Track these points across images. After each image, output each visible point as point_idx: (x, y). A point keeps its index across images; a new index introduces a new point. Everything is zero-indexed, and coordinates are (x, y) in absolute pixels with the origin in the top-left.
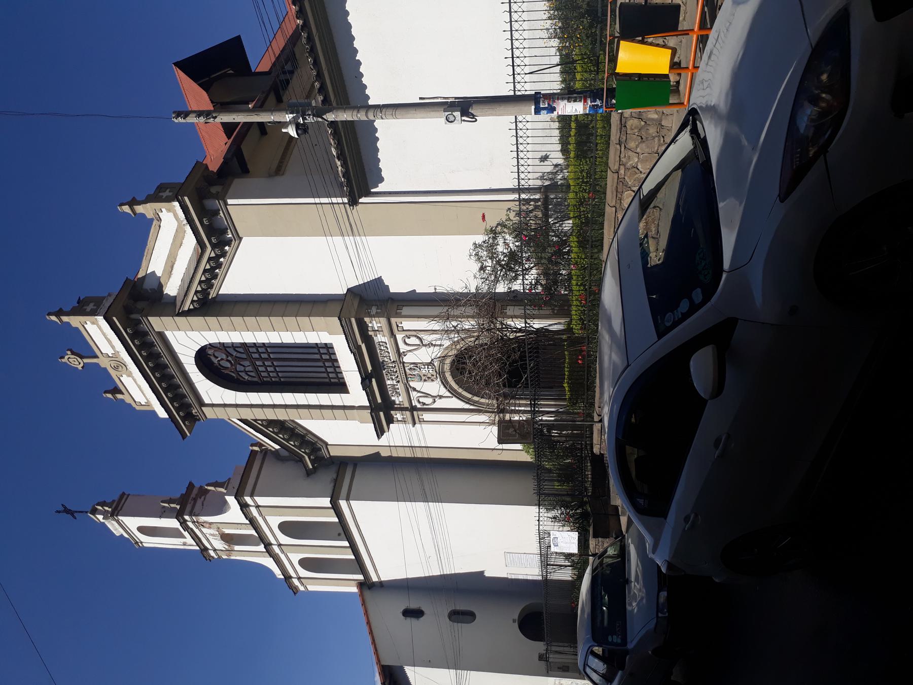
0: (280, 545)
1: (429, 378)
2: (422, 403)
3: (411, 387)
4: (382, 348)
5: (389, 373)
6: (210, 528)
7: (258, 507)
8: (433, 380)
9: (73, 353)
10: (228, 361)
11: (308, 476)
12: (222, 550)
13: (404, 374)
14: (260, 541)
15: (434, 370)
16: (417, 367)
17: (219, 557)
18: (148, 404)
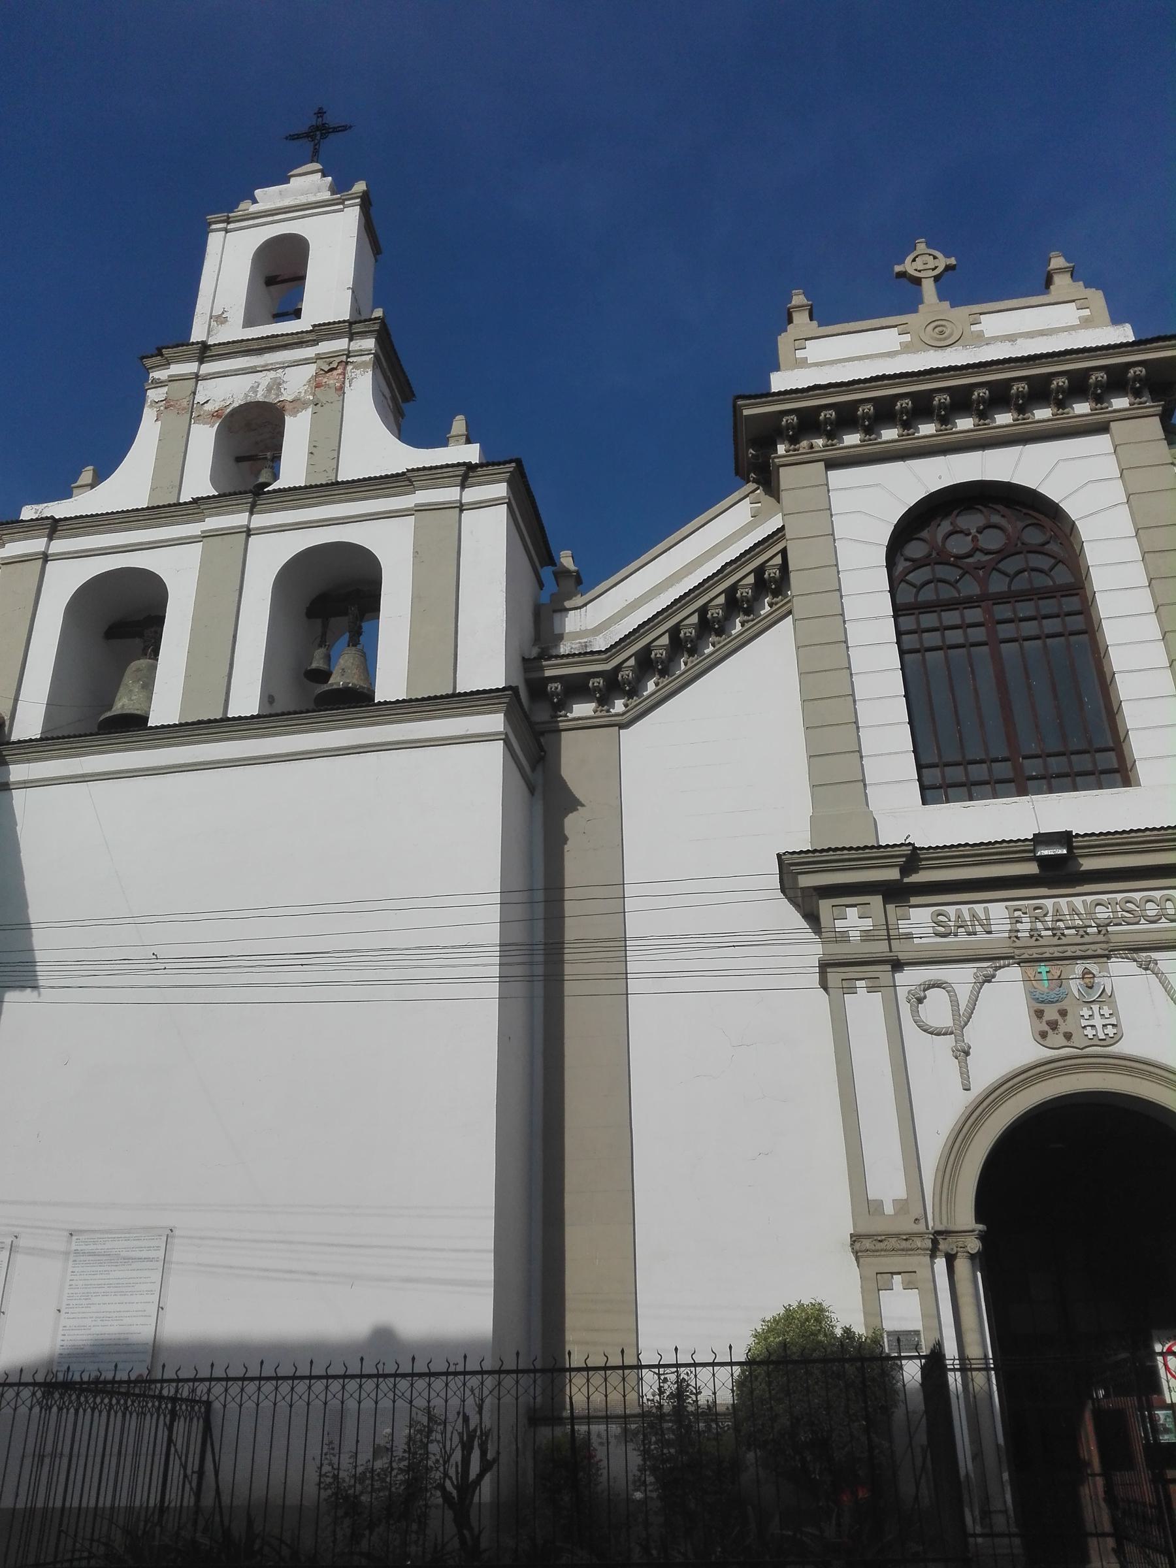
0: (249, 532)
1: (1053, 1025)
2: (925, 997)
3: (1000, 967)
4: (1152, 910)
5: (1047, 913)
6: (316, 384)
7: (461, 507)
8: (1044, 1035)
9: (948, 268)
10: (976, 549)
11: (523, 658)
12: (194, 393)
13: (1057, 955)
14: (221, 493)
15: (1096, 1042)
16: (1100, 996)
17: (159, 384)
18: (803, 363)
